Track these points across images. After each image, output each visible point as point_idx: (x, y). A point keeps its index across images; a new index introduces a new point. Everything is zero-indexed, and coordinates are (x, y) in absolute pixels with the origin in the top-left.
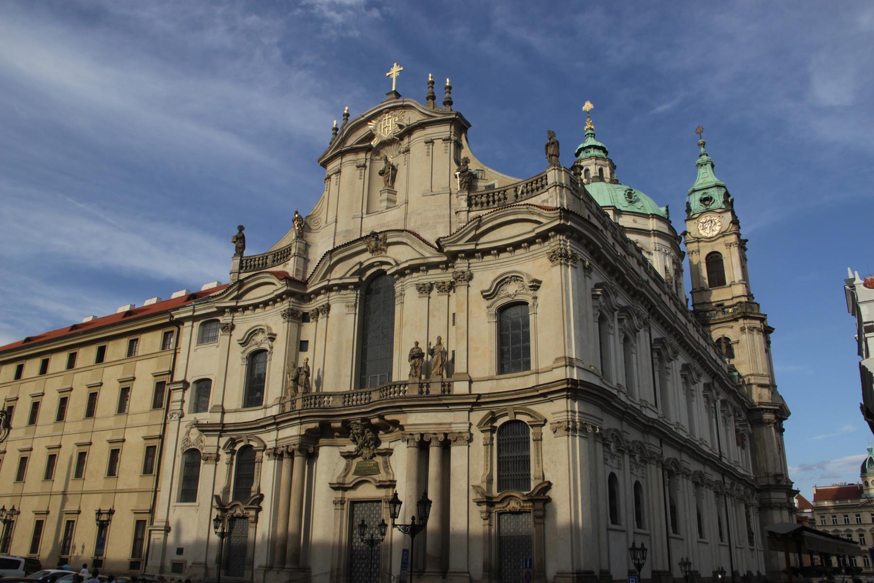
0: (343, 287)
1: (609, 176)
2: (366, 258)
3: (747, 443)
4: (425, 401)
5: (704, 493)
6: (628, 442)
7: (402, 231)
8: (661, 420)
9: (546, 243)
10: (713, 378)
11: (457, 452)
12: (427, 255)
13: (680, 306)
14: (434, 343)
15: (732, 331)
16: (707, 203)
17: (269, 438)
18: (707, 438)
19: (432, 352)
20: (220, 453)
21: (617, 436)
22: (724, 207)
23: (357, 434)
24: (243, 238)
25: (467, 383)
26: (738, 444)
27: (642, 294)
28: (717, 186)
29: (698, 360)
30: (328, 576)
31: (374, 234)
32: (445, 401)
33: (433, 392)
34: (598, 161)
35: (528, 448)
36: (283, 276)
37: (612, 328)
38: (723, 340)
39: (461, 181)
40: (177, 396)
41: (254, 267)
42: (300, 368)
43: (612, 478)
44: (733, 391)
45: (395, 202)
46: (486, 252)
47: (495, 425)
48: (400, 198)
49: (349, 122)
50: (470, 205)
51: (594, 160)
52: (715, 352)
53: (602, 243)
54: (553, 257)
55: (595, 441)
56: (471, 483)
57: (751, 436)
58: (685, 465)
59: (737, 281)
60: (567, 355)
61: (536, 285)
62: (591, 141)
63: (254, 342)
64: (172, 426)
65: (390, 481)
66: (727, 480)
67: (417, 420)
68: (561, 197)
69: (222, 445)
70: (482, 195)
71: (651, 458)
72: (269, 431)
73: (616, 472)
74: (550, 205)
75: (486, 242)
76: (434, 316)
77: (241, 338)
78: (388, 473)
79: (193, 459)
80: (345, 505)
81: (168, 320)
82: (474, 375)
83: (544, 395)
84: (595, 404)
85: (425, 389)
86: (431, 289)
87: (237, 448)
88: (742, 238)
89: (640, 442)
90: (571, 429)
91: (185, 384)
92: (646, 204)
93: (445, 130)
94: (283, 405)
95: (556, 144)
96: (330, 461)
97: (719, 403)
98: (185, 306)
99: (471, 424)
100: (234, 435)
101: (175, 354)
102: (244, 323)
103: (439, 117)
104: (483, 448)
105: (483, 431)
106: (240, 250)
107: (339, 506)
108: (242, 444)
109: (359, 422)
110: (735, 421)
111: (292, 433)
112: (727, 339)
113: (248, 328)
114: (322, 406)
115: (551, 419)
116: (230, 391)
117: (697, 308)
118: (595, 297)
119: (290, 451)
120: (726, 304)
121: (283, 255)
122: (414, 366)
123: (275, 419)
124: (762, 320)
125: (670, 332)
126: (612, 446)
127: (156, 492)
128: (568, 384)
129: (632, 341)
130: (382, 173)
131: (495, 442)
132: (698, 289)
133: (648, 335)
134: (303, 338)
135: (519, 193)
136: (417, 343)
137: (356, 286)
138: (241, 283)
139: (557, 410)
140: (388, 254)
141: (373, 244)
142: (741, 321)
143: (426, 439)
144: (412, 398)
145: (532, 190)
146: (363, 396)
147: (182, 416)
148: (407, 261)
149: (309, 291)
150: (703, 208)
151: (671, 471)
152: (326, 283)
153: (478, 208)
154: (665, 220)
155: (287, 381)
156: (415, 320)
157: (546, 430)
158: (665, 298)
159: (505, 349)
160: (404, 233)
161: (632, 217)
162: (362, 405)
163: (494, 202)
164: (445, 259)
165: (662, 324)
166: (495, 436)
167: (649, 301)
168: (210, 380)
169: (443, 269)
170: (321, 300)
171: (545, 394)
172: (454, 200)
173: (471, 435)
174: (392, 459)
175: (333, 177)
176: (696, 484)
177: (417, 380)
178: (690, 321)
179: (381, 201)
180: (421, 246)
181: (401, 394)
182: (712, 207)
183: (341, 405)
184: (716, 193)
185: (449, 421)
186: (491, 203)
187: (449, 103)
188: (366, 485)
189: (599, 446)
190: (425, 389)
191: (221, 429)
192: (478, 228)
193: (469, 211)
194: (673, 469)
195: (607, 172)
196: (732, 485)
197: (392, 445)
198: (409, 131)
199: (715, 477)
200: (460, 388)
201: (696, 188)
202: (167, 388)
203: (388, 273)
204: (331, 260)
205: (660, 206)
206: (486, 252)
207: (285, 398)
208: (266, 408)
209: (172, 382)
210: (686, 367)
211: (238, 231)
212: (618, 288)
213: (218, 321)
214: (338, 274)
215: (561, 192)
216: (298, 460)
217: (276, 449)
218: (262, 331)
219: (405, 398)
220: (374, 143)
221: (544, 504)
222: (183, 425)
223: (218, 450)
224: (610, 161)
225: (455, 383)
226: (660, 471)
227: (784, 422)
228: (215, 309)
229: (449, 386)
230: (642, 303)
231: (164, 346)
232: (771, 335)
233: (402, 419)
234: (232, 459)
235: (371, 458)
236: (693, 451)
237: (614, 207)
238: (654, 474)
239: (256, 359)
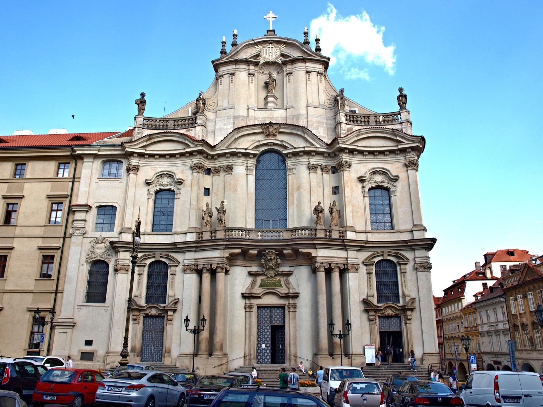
0: (246, 155)
11: (351, 276)
12: (318, 146)
17: (188, 258)
30: (242, 360)
31: (271, 124)
32: (343, 244)
40: (79, 216)
46: (361, 152)
61: (395, 179)
72: (184, 252)
81: (69, 154)
82: (358, 228)
87: (148, 262)
91: (87, 208)
93: (320, 68)
94: (200, 234)
95: (405, 96)
101: (73, 182)
105: (366, 265)
106: (141, 110)
107: (248, 310)
108: (153, 260)
109: (274, 251)
111: (216, 255)
127: (56, 292)
130: (267, 84)
131: (374, 271)
136: (319, 203)
143: (333, 266)
144: (321, 239)
152: (234, 150)
157: (409, 268)
160: (300, 129)
166: (373, 267)
168: (114, 208)
169: (326, 157)
170: (223, 162)
180: (314, 140)
183: (256, 238)
187: (318, 49)
197: (291, 269)
198: (294, 61)
206: (361, 152)
233: (313, 252)
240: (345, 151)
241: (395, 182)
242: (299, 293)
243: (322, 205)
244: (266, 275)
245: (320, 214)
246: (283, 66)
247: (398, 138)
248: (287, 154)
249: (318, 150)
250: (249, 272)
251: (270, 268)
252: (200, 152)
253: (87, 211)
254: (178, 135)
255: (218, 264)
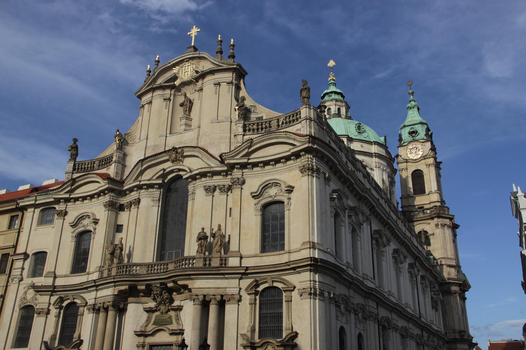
0: (151, 186)
1: (345, 114)
2: (168, 166)
3: (440, 308)
4: (208, 271)
5: (408, 343)
6: (354, 304)
7: (195, 147)
8: (377, 289)
9: (298, 160)
10: (415, 260)
11: (230, 309)
12: (213, 165)
13: (392, 208)
14: (216, 229)
15: (429, 227)
16: (413, 135)
17: (90, 297)
18: (411, 303)
19: (214, 236)
20: (50, 308)
21: (346, 300)
22: (425, 138)
23: (157, 294)
24: (77, 147)
25: (239, 258)
26: (433, 308)
27: (365, 198)
28: (421, 123)
29: (405, 247)
31: (174, 149)
32: (222, 271)
33: (213, 265)
34: (337, 103)
35: (281, 307)
36: (106, 177)
37: (343, 222)
38: (423, 233)
39: (239, 113)
40: (18, 264)
41: (85, 170)
42: (116, 245)
43: (342, 330)
44: (430, 269)
45: (191, 126)
46: (255, 165)
47: (258, 289)
48: (194, 123)
49: (159, 67)
50: (245, 131)
51: (334, 102)
52: (417, 241)
53: (338, 161)
54: (303, 170)
55: (330, 303)
56: (240, 332)
57: (442, 302)
58: (394, 322)
59: (433, 191)
60: (311, 240)
61: (290, 190)
62: (333, 88)
63: (82, 225)
64: (13, 287)
65: (180, 330)
66: (425, 334)
67: (202, 285)
68: (310, 127)
69: (52, 302)
70: (254, 124)
71: (370, 316)
72: (90, 292)
73: (344, 326)
74: (302, 132)
75: (256, 157)
76: (217, 210)
77: (72, 221)
78: (178, 324)
79: (28, 313)
80: (146, 348)
81: (14, 207)
82: (244, 253)
83: (294, 269)
84: (331, 276)
85: (208, 262)
86: (214, 190)
87: (64, 304)
88: (438, 160)
89: (362, 305)
90: (313, 294)
91: (26, 256)
92: (371, 134)
93: (229, 76)
94: (102, 272)
96: (135, 314)
97: (419, 278)
98: (28, 197)
99: (240, 289)
100: (63, 294)
102: (74, 211)
103: (225, 66)
104: (249, 306)
105: (249, 294)
106: (74, 157)
108: (69, 301)
109: (158, 285)
110: (431, 291)
111: (107, 293)
112: (426, 232)
113: (78, 214)
114: (131, 273)
115: (298, 286)
116: (61, 261)
117: (404, 209)
118: (332, 199)
119: (105, 306)
120: (426, 207)
121: (106, 162)
122: (200, 246)
123: (95, 282)
124: (451, 219)
125: (385, 226)
126: (342, 307)
128: (311, 261)
129: (358, 231)
130: (182, 105)
131: (258, 302)
132: (406, 196)
133: (369, 227)
134: (119, 223)
135: (280, 123)
136: (203, 229)
137: (160, 186)
138: (74, 181)
139: (303, 280)
140: (184, 164)
141: (174, 156)
142: (436, 219)
143: (207, 299)
144: (198, 269)
145: (290, 122)
146: (162, 267)
147: (21, 280)
148: (198, 169)
149: (125, 188)
150: (410, 139)
151: (384, 327)
152: (138, 183)
153: (250, 133)
154: (383, 146)
155: (105, 254)
156: (202, 212)
157: (295, 294)
158: (382, 202)
159: (267, 234)
160: (197, 149)
161: (360, 144)
162: (161, 273)
163: (262, 129)
164: (225, 168)
165: (380, 220)
166: (258, 297)
167: (371, 204)
168: (46, 253)
169: (224, 176)
170: (134, 195)
171: (294, 268)
172: (234, 127)
173: (241, 296)
174: (182, 313)
175: (146, 106)
176: (403, 337)
177: (202, 255)
178: (399, 218)
179: (181, 125)
180: (208, 159)
181: (190, 266)
182: (417, 138)
183: (145, 272)
184: (420, 128)
185: (224, 286)
186: (260, 130)
188: (162, 333)
189: (333, 307)
190: (208, 262)
191: (53, 290)
192: (250, 148)
193: (244, 135)
194: (386, 324)
195: (343, 111)
196: (429, 337)
197: (182, 303)
198: (202, 76)
199: (416, 331)
200: (233, 262)
201: (406, 123)
202: (10, 259)
203: (184, 177)
204: (142, 166)
205: (380, 136)
206: (255, 165)
207: (103, 267)
208: (88, 274)
209: (15, 254)
210: (396, 251)
211: (73, 142)
212: (348, 193)
213: (55, 208)
214: (147, 177)
215: (310, 124)
216: (111, 313)
217: (94, 305)
218: (89, 217)
219: (193, 269)
220: (177, 83)
221: (292, 348)
222: (21, 287)
223: (49, 306)
224: (346, 103)
225: (230, 258)
226: (377, 325)
227: (466, 293)
228: (53, 200)
229: (226, 260)
230: (366, 204)
231: (10, 226)
232: (457, 230)
233: (191, 284)
234: (60, 313)
235: (167, 312)
236: (401, 312)
237: (348, 135)
238: (372, 328)
239: (83, 239)
240: (236, 166)
241: (289, 193)
242: (184, 330)
243: (204, 231)
244: (159, 310)
245: (200, 241)
246: (197, 83)
247: (291, 141)
248: (187, 178)
249: (212, 170)
250: (144, 308)
251: (160, 303)
252: (110, 190)
253: (25, 259)
254: (95, 176)
255: (109, 302)
